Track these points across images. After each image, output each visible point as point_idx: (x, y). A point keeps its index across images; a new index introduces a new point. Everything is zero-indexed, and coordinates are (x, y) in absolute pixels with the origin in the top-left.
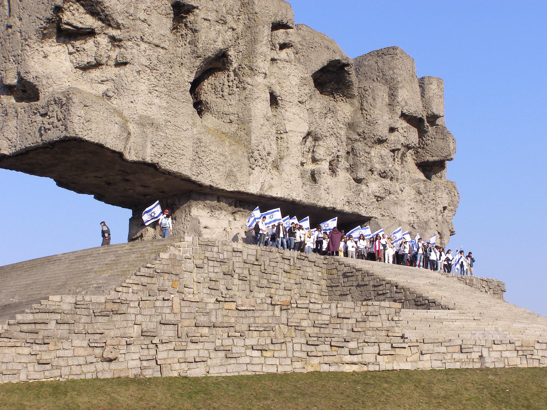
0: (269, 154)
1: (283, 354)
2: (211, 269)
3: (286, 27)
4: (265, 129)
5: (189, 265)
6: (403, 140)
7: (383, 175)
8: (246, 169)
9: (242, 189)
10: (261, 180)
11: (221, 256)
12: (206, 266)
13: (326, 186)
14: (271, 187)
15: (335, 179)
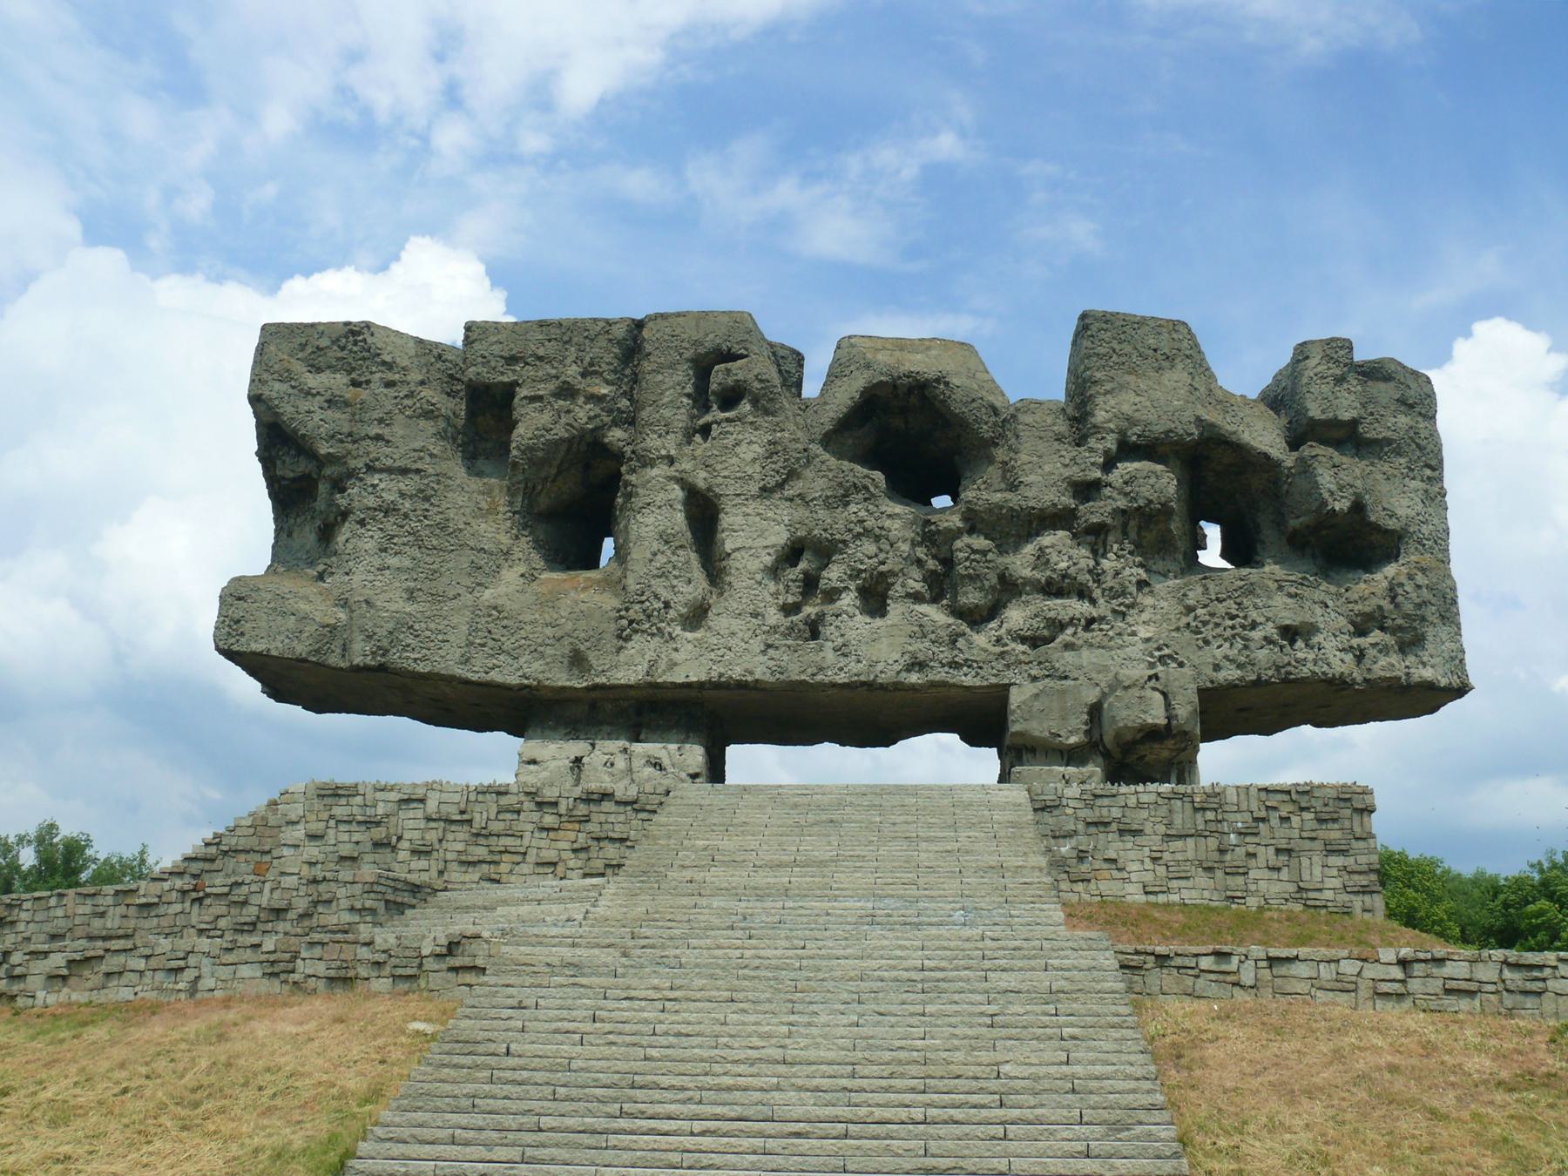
0: (667, 605)
2: (345, 837)
3: (732, 357)
4: (661, 559)
5: (298, 833)
6: (1122, 503)
7: (1053, 589)
8: (610, 642)
9: (601, 680)
10: (650, 655)
11: (369, 811)
12: (331, 832)
13: (840, 641)
14: (673, 665)
15: (878, 622)
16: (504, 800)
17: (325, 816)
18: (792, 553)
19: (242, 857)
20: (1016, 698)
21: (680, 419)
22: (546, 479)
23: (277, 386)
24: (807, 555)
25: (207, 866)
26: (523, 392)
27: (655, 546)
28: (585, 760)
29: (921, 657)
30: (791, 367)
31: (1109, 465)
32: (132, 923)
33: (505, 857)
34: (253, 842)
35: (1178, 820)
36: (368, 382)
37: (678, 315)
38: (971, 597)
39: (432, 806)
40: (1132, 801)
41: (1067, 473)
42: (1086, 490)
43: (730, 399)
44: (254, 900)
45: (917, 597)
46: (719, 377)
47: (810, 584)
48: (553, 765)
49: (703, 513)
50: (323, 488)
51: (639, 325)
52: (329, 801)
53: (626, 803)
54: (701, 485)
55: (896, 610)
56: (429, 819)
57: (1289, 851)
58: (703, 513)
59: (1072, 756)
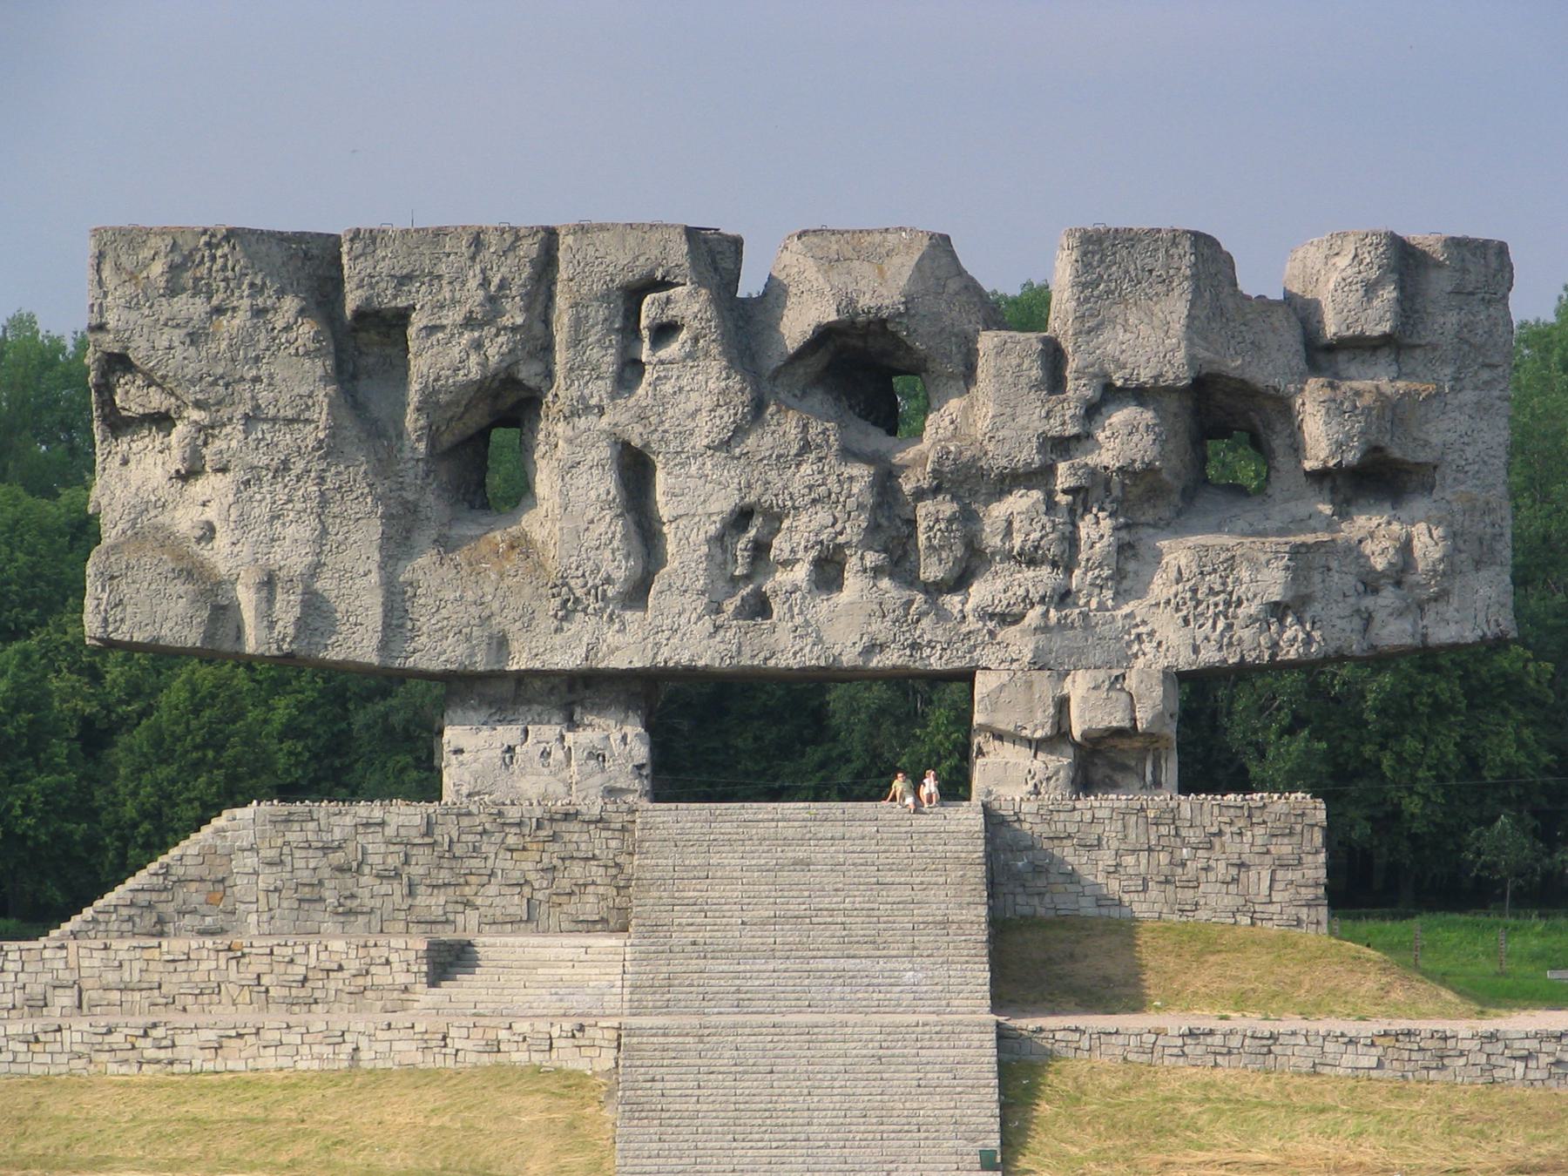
1: (57, 1047)
3: (664, 285)
11: (326, 837)
16: (465, 822)
17: (280, 842)
18: (742, 517)
19: (193, 886)
20: (984, 684)
21: (609, 362)
22: (451, 418)
23: (125, 314)
24: (758, 521)
25: (154, 897)
26: (418, 321)
27: (591, 513)
28: (518, 749)
29: (881, 638)
30: (727, 264)
31: (1092, 411)
32: (156, 978)
33: (472, 879)
34: (203, 871)
35: (1132, 836)
36: (234, 309)
37: (602, 228)
38: (932, 571)
39: (390, 831)
40: (1088, 816)
41: (1042, 427)
42: (1060, 446)
43: (665, 331)
44: (298, 960)
45: (877, 572)
46: (649, 309)
47: (760, 549)
48: (484, 756)
49: (635, 469)
50: (180, 429)
51: (551, 235)
52: (281, 827)
53: (589, 822)
54: (637, 442)
55: (854, 584)
56: (388, 842)
57: (1241, 865)
58: (635, 469)
59: (1037, 745)
